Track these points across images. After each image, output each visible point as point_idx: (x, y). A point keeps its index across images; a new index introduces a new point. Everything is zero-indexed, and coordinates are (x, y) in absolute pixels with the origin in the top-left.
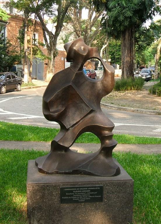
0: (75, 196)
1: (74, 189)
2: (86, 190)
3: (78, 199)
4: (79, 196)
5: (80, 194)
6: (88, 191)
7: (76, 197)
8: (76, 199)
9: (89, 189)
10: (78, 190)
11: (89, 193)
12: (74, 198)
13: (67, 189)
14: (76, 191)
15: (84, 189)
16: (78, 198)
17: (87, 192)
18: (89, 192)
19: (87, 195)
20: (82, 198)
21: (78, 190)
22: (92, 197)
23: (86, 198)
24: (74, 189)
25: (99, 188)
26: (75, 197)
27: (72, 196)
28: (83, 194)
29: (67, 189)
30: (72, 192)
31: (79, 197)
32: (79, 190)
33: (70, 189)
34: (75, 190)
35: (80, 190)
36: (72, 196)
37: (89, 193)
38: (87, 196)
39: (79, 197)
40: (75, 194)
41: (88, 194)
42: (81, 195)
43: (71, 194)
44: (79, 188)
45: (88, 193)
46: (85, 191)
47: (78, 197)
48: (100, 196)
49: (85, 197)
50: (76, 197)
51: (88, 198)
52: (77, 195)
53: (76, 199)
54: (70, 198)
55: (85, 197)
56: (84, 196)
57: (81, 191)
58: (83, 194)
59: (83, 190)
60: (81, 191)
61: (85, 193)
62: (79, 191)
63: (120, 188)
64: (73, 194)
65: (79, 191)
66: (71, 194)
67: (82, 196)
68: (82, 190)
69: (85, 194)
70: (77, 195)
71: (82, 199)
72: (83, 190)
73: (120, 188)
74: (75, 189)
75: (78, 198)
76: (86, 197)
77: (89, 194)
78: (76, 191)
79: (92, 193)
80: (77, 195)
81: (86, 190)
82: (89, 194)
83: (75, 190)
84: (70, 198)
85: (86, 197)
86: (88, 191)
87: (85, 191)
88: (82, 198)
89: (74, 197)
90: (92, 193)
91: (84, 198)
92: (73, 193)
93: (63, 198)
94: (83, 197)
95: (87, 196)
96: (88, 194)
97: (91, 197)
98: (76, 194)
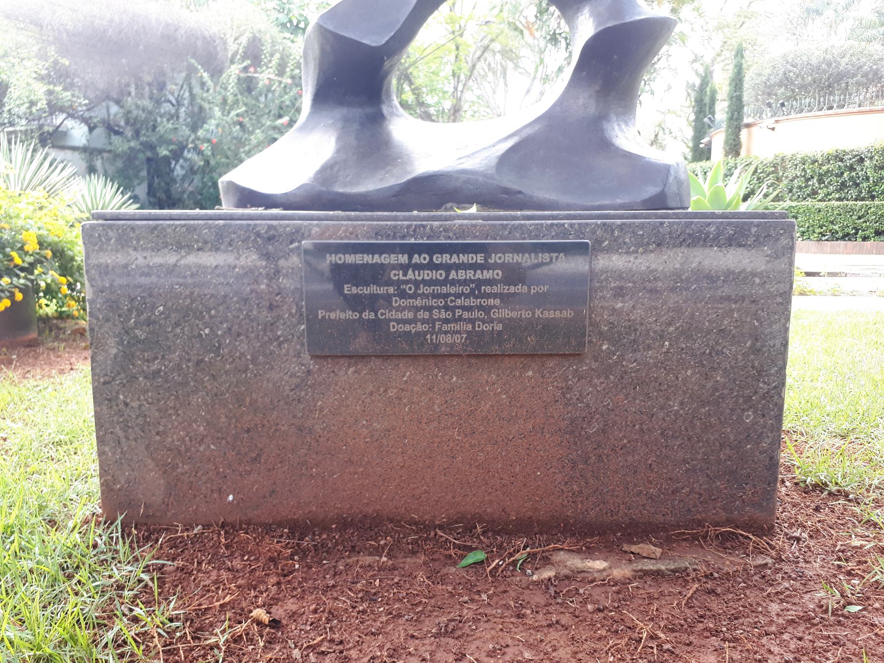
0: (403, 302)
2: (474, 267)
3: (420, 327)
4: (429, 309)
6: (487, 275)
7: (410, 315)
8: (407, 328)
10: (419, 267)
11: (495, 289)
12: (398, 321)
15: (464, 258)
16: (424, 321)
17: (480, 283)
18: (491, 282)
19: (484, 302)
20: (446, 321)
21: (419, 267)
22: (514, 314)
23: (472, 321)
26: (400, 309)
28: (458, 296)
31: (426, 315)
32: (432, 266)
33: (368, 259)
34: (405, 268)
35: (437, 267)
37: (495, 289)
38: (480, 308)
39: (426, 315)
40: (403, 295)
41: (488, 296)
42: (441, 302)
44: (431, 249)
45: (488, 289)
46: (470, 274)
49: (466, 315)
51: (491, 321)
52: (418, 302)
53: (407, 328)
54: (368, 315)
55: (466, 315)
56: (464, 308)
57: (440, 275)
58: (458, 296)
59: (458, 267)
60: (440, 275)
61: (467, 290)
62: (427, 275)
64: (391, 290)
65: (427, 275)
66: (374, 289)
67: (446, 308)
68: (448, 268)
69: (467, 296)
70: (414, 296)
71: (445, 327)
72: (458, 267)
74: (403, 259)
75: (424, 321)
76: (477, 314)
77: (495, 296)
78: (410, 275)
79: (512, 289)
80: (418, 302)
81: (474, 267)
82: (495, 296)
85: (477, 314)
86: (487, 275)
87: (470, 274)
88: (446, 321)
89: (400, 316)
90: (512, 289)
91: (460, 319)
92: (390, 282)
94: (458, 312)
95: (480, 308)
96: (488, 296)
97: (506, 313)
98: (410, 289)
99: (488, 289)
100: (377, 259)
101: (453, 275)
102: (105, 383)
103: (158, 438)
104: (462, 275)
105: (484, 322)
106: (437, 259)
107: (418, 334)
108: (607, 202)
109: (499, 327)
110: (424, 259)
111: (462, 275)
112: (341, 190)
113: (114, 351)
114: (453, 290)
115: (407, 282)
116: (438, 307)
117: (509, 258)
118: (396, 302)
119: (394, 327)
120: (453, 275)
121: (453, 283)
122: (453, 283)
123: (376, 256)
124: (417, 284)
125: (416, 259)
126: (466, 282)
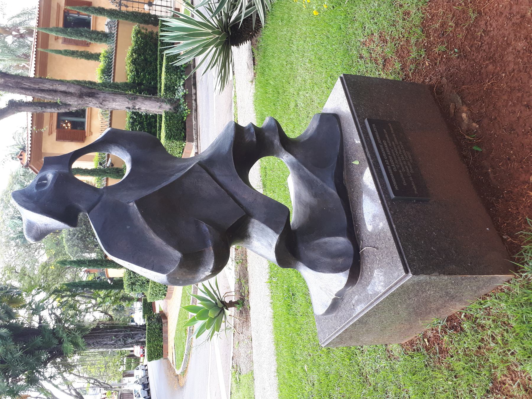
1: (390, 170)
2: (385, 148)
3: (409, 164)
7: (406, 167)
9: (380, 142)
10: (390, 162)
12: (410, 170)
16: (407, 162)
20: (404, 156)
21: (390, 162)
23: (402, 150)
24: (390, 170)
26: (405, 169)
29: (395, 183)
32: (388, 159)
38: (396, 147)
40: (400, 168)
46: (387, 149)
47: (405, 162)
49: (400, 151)
52: (402, 164)
54: (411, 179)
57: (391, 158)
58: (395, 153)
59: (386, 152)
60: (391, 158)
62: (392, 161)
65: (392, 161)
67: (400, 156)
68: (387, 155)
69: (394, 151)
71: (406, 157)
72: (386, 152)
74: (389, 167)
80: (402, 164)
85: (399, 148)
99: (390, 145)
101: (389, 154)
102: (466, 270)
103: (478, 252)
104: (388, 151)
105: (400, 147)
107: (411, 164)
108: (339, 129)
109: (401, 143)
111: (388, 151)
112: (346, 221)
113: (454, 266)
114: (394, 154)
115: (396, 167)
116: (401, 159)
117: (378, 139)
119: (412, 171)
120: (389, 154)
121: (391, 154)
122: (391, 154)
123: (391, 175)
125: (388, 163)
126: (390, 150)
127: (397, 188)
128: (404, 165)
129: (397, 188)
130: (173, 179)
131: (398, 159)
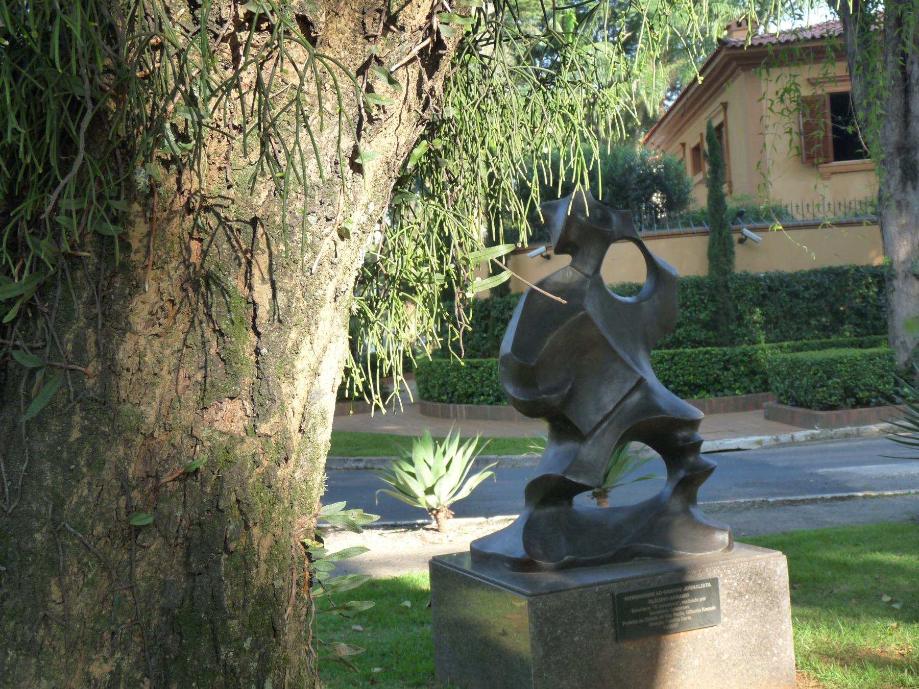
4: (663, 614)
5: (665, 608)
7: (656, 618)
10: (658, 597)
13: (633, 597)
14: (656, 601)
25: (709, 585)
26: (653, 616)
27: (646, 614)
29: (633, 597)
30: (644, 602)
32: (663, 595)
34: (652, 598)
36: (646, 614)
40: (653, 610)
43: (643, 609)
47: (661, 617)
48: (713, 608)
50: (656, 618)
51: (686, 615)
52: (659, 612)
53: (656, 624)
54: (641, 621)
63: (755, 580)
66: (643, 609)
70: (657, 610)
73: (755, 580)
74: (652, 594)
80: (659, 612)
83: (652, 598)
84: (641, 621)
92: (648, 605)
93: (624, 623)
98: (655, 607)
100: (642, 596)
106: (665, 592)
110: (659, 593)
118: (651, 613)
119: (651, 625)
124: (658, 604)
127: (626, 599)
128: (658, 615)
129: (626, 599)
130: (620, 351)
131: (665, 608)
